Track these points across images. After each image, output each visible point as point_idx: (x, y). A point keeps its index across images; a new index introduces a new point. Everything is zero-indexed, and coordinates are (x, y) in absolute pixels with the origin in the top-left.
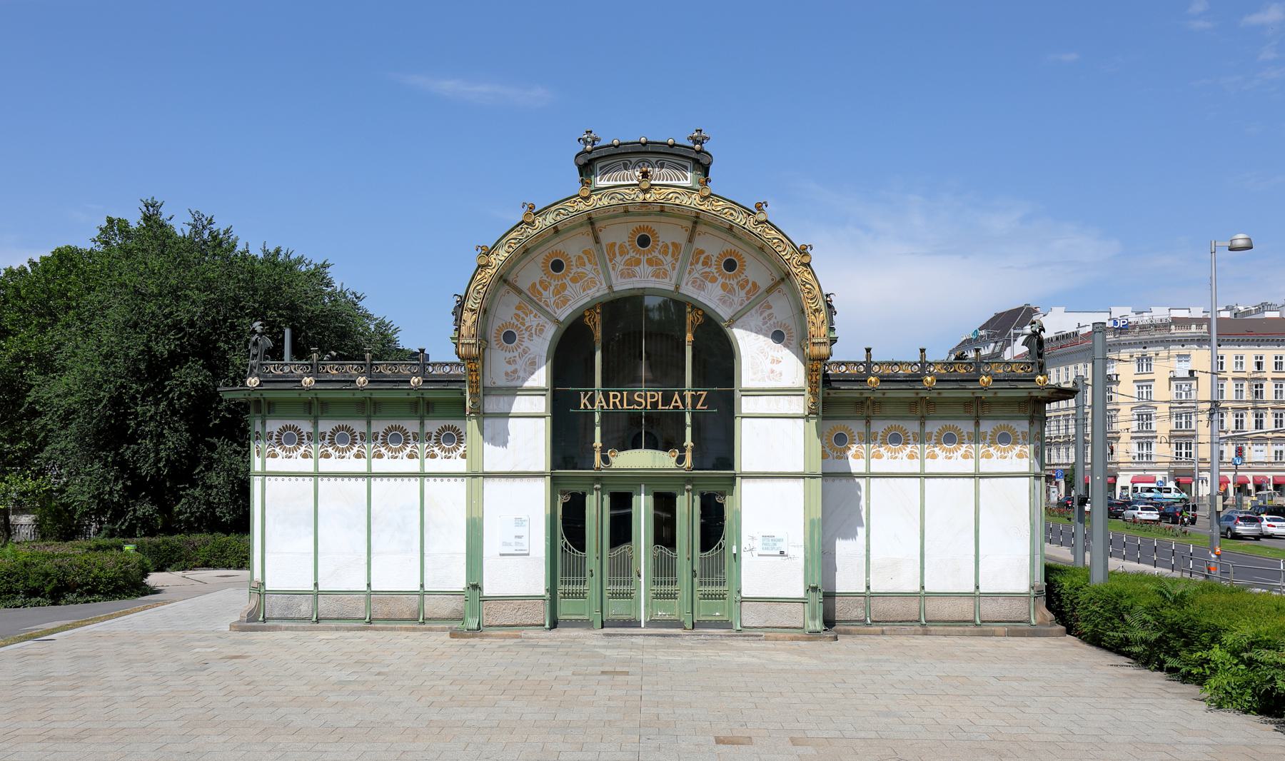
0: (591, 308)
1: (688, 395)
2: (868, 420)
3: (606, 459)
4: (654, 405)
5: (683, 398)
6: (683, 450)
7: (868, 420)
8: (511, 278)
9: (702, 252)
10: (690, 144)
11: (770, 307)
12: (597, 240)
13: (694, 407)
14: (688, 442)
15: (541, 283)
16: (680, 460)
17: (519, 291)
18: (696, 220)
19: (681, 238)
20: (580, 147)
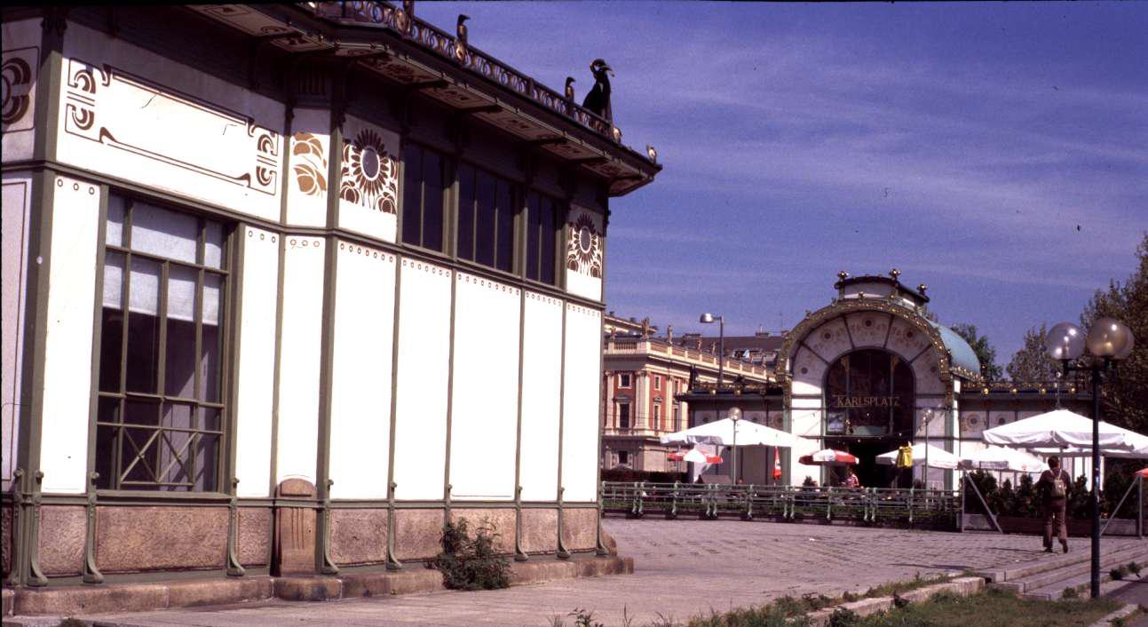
0: (844, 356)
1: (891, 398)
2: (988, 412)
3: (851, 431)
4: (873, 404)
5: (888, 401)
6: (888, 427)
7: (988, 412)
8: (805, 342)
9: (895, 329)
10: (890, 277)
11: (928, 355)
12: (846, 324)
13: (893, 403)
14: (891, 423)
15: (820, 344)
16: (888, 431)
17: (809, 349)
18: (893, 317)
19: (887, 324)
20: (838, 279)
